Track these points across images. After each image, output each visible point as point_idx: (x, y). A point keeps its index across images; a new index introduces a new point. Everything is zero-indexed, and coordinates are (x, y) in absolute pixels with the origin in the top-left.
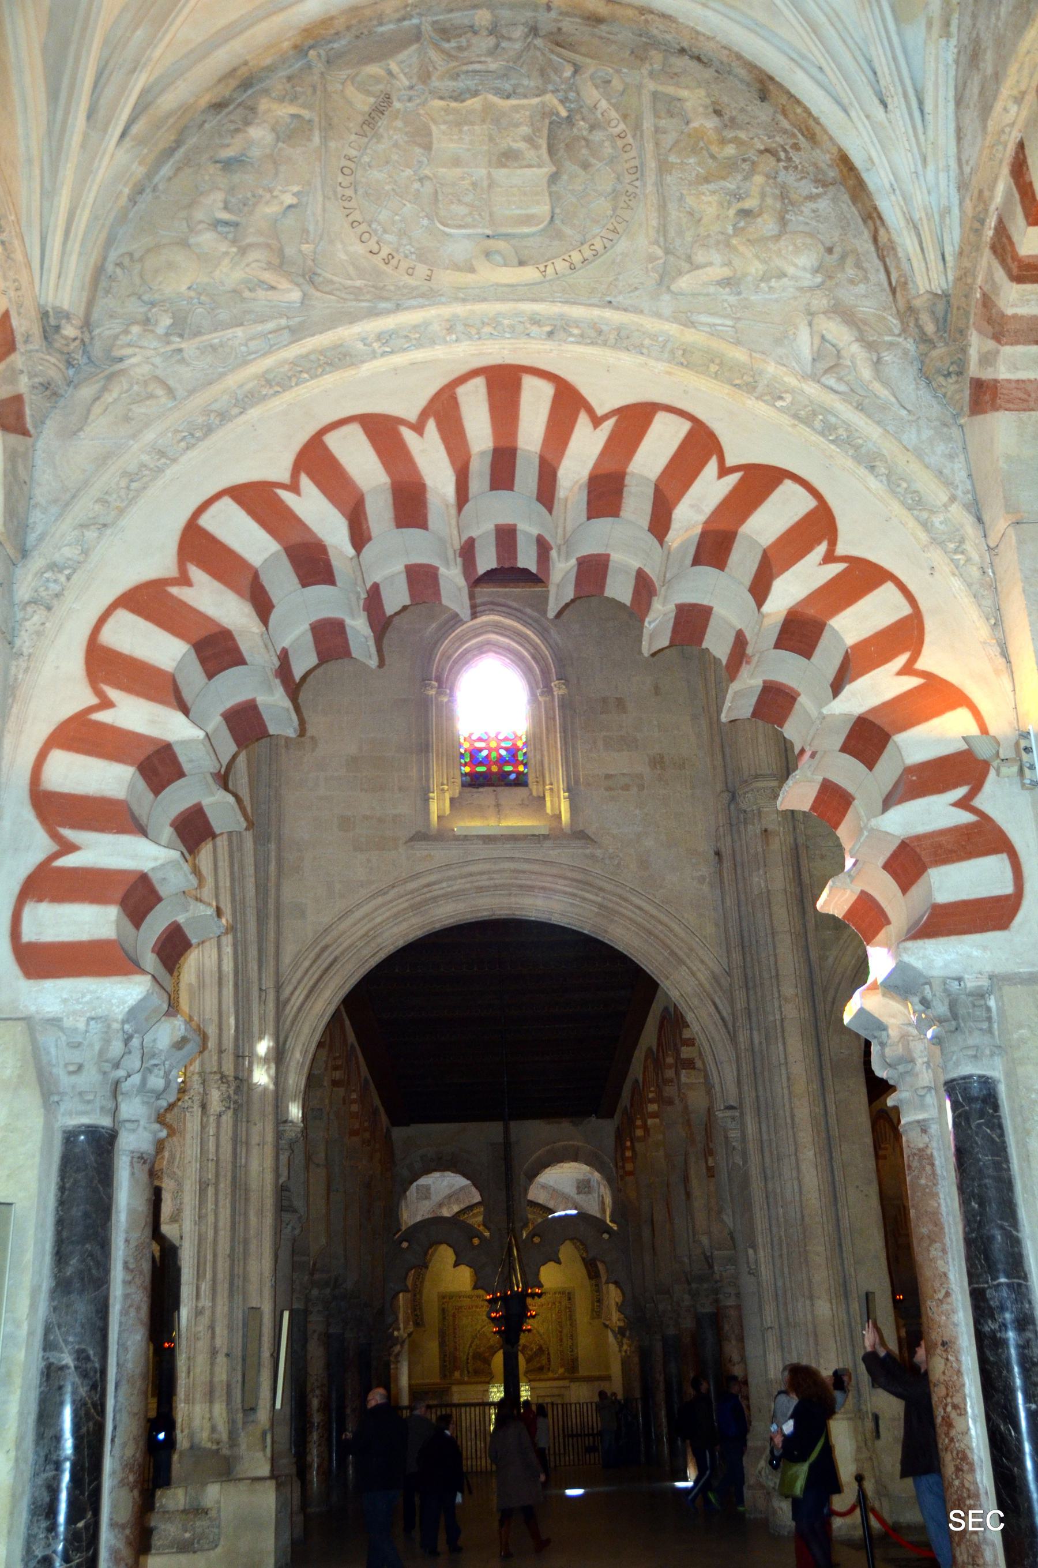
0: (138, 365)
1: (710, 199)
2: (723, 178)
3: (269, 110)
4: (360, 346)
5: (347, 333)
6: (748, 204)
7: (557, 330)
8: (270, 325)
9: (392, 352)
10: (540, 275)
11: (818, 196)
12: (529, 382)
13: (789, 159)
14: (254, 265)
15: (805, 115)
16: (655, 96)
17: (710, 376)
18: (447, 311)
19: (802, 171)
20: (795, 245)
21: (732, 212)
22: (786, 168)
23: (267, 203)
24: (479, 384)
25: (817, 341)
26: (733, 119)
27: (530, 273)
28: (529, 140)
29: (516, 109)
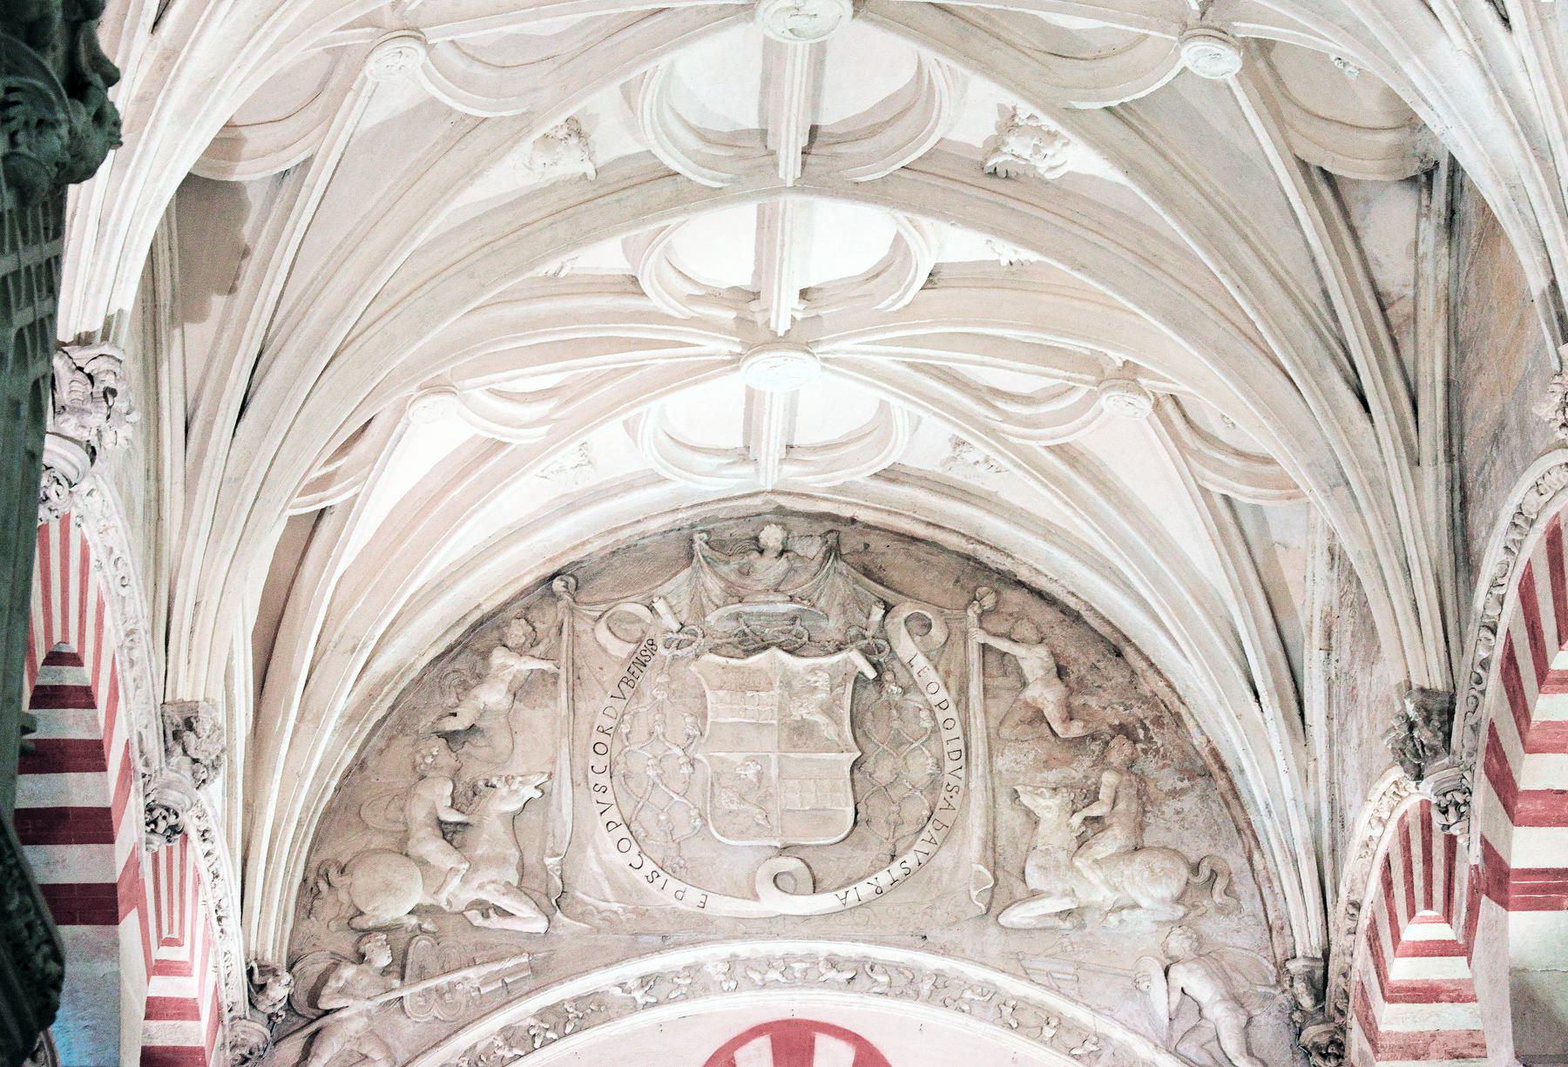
0: (349, 1019)
1: (1049, 803)
2: (1068, 763)
3: (504, 667)
4: (618, 991)
5: (599, 980)
6: (1096, 810)
7: (859, 974)
8: (509, 964)
9: (657, 1003)
10: (839, 903)
11: (1183, 791)
12: (823, 1043)
13: (1149, 739)
14: (489, 887)
15: (1167, 690)
16: (985, 648)
17: (1045, 1043)
18: (724, 950)
19: (1164, 757)
20: (1152, 870)
21: (1077, 820)
22: (1145, 751)
23: (502, 799)
24: (763, 1043)
25: (1176, 996)
26: (1080, 680)
27: (826, 902)
28: (828, 710)
29: (813, 670)
